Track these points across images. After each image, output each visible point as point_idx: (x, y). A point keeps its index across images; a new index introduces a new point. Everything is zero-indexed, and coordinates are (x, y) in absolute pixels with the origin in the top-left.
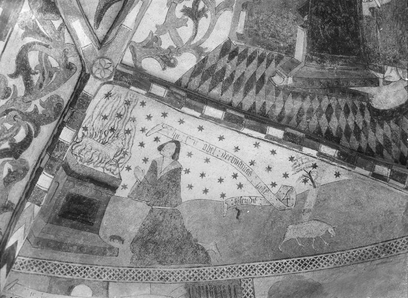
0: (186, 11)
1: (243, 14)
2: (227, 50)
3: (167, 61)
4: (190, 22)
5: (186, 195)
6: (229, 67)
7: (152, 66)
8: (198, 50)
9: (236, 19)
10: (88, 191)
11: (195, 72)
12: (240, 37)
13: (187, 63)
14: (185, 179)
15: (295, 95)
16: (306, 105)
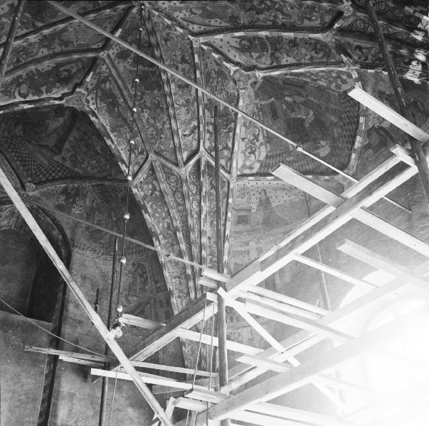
0: (249, 153)
1: (268, 145)
2: (267, 157)
3: (251, 168)
4: (253, 155)
5: (274, 205)
6: (271, 162)
7: (247, 171)
8: (259, 161)
9: (266, 147)
10: (243, 213)
11: (260, 168)
12: (270, 152)
13: (257, 166)
14: (271, 200)
15: (295, 162)
16: (300, 164)
